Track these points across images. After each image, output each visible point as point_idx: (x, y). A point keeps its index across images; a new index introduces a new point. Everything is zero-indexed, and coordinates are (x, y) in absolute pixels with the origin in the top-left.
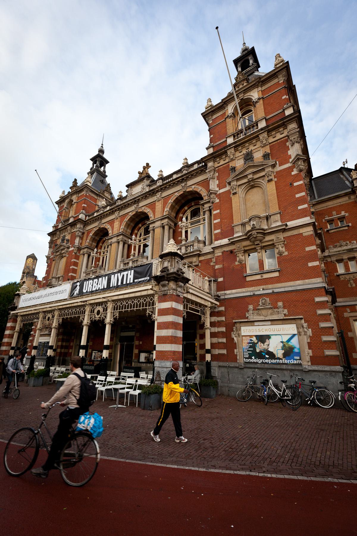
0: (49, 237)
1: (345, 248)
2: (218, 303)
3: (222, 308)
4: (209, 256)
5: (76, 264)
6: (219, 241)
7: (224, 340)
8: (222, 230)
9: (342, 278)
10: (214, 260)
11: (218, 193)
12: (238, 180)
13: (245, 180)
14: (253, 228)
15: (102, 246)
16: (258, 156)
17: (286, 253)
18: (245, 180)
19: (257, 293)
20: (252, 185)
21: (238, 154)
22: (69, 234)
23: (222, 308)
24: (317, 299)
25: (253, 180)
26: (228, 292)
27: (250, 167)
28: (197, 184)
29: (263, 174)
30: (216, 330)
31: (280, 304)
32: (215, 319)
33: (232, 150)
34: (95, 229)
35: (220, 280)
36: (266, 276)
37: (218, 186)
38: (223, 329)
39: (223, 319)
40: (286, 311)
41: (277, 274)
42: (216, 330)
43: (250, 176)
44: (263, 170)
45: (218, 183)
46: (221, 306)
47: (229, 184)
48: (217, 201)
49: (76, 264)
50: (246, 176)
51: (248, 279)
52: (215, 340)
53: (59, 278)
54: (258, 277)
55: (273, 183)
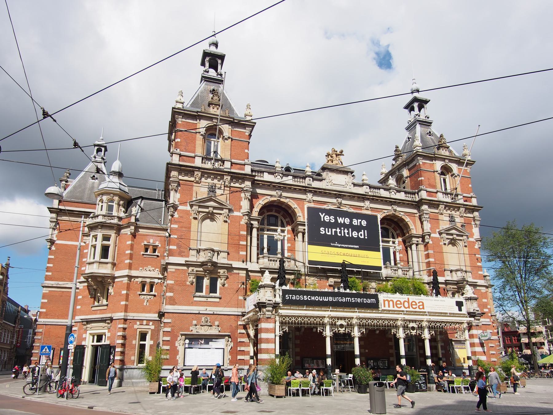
12: (447, 234)
13: (451, 237)
18: (451, 237)
37: (431, 229)
43: (455, 236)
44: (462, 236)
50: (452, 235)
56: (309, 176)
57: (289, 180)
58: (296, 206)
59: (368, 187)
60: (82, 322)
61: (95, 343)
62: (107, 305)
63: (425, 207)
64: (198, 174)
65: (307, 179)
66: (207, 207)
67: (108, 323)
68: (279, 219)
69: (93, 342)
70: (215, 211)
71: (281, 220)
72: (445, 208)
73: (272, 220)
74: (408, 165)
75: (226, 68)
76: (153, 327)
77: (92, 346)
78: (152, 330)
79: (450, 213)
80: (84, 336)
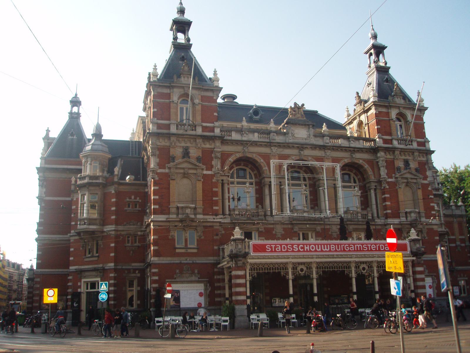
8: (392, 211)
11: (387, 181)
17: (427, 238)
22: (199, 148)
28: (364, 160)
29: (415, 181)
33: (398, 152)
34: (238, 155)
37: (387, 174)
43: (410, 180)
45: (386, 172)
48: (387, 187)
50: (407, 178)
56: (274, 132)
58: (262, 161)
59: (328, 138)
60: (77, 271)
61: (89, 290)
62: (98, 256)
64: (173, 139)
65: (272, 134)
67: (100, 272)
68: (248, 172)
69: (87, 289)
71: (250, 173)
72: (400, 153)
73: (241, 173)
74: (367, 113)
75: (192, 33)
76: (139, 275)
77: (87, 292)
78: (138, 277)
79: (405, 158)
80: (79, 284)
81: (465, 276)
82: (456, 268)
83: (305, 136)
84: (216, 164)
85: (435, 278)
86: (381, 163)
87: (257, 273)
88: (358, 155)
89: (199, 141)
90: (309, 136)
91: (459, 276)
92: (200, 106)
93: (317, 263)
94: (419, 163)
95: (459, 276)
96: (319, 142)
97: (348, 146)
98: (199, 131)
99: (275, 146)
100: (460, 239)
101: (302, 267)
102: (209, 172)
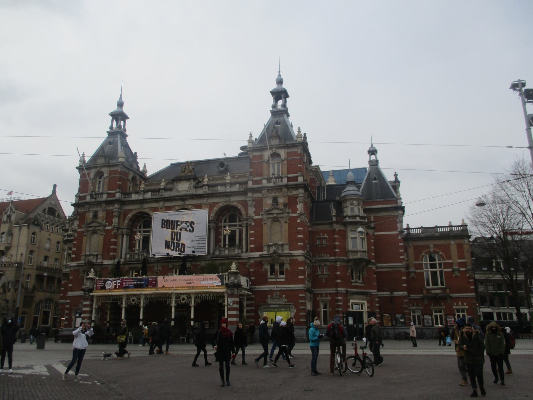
0: (73, 208)
1: (323, 258)
2: (251, 293)
3: (254, 296)
4: (245, 261)
5: (115, 244)
6: (253, 253)
7: (254, 314)
9: (320, 277)
10: (249, 264)
12: (268, 214)
14: (275, 252)
15: (137, 226)
16: (281, 200)
19: (273, 289)
20: (276, 220)
21: (269, 194)
22: (104, 211)
23: (254, 296)
24: (300, 295)
25: (277, 217)
26: (257, 287)
27: (275, 208)
29: (282, 215)
30: (249, 308)
31: (284, 296)
32: (249, 302)
33: (266, 191)
34: (135, 212)
35: (253, 278)
36: (278, 280)
37: (255, 212)
38: (254, 308)
39: (254, 302)
40: (286, 300)
41: (283, 280)
42: (249, 308)
43: (275, 215)
44: (283, 213)
46: (253, 294)
47: (262, 215)
48: (253, 224)
49: (115, 244)
50: (273, 214)
51: (269, 280)
52: (248, 314)
53: (97, 255)
54: (274, 280)
55: (287, 224)
57: (149, 195)
63: (250, 194)
66: (92, 227)
70: (97, 228)
81: (465, 304)
82: (451, 295)
83: (187, 189)
84: (115, 220)
85: (294, 307)
86: (249, 203)
87: (101, 303)
88: (233, 199)
89: (104, 205)
90: (190, 188)
91: (455, 304)
92: (108, 178)
93: (145, 294)
94: (288, 197)
95: (455, 304)
96: (200, 192)
97: (224, 191)
98: (105, 197)
99: (161, 201)
100: (459, 263)
101: (135, 298)
102: (110, 228)
